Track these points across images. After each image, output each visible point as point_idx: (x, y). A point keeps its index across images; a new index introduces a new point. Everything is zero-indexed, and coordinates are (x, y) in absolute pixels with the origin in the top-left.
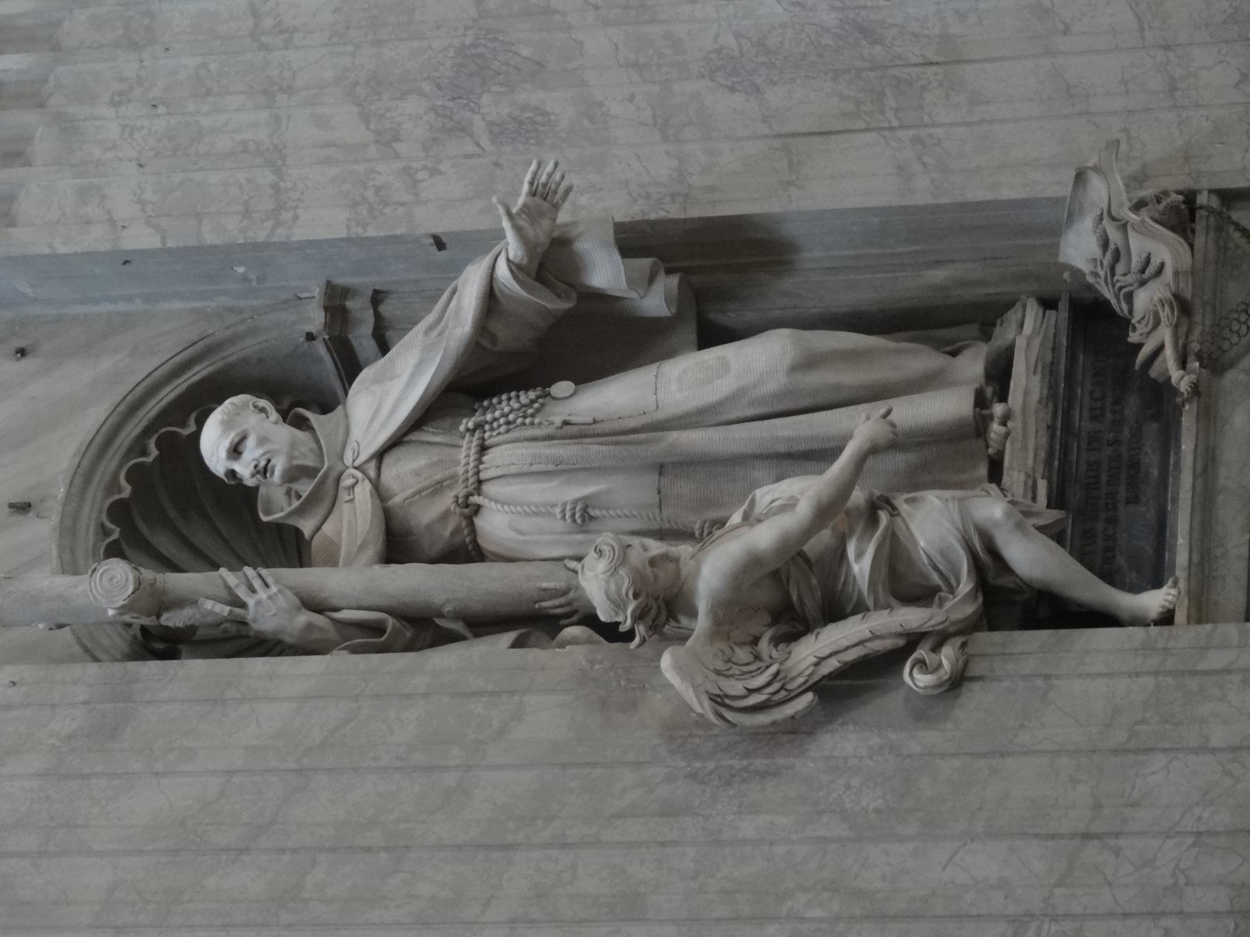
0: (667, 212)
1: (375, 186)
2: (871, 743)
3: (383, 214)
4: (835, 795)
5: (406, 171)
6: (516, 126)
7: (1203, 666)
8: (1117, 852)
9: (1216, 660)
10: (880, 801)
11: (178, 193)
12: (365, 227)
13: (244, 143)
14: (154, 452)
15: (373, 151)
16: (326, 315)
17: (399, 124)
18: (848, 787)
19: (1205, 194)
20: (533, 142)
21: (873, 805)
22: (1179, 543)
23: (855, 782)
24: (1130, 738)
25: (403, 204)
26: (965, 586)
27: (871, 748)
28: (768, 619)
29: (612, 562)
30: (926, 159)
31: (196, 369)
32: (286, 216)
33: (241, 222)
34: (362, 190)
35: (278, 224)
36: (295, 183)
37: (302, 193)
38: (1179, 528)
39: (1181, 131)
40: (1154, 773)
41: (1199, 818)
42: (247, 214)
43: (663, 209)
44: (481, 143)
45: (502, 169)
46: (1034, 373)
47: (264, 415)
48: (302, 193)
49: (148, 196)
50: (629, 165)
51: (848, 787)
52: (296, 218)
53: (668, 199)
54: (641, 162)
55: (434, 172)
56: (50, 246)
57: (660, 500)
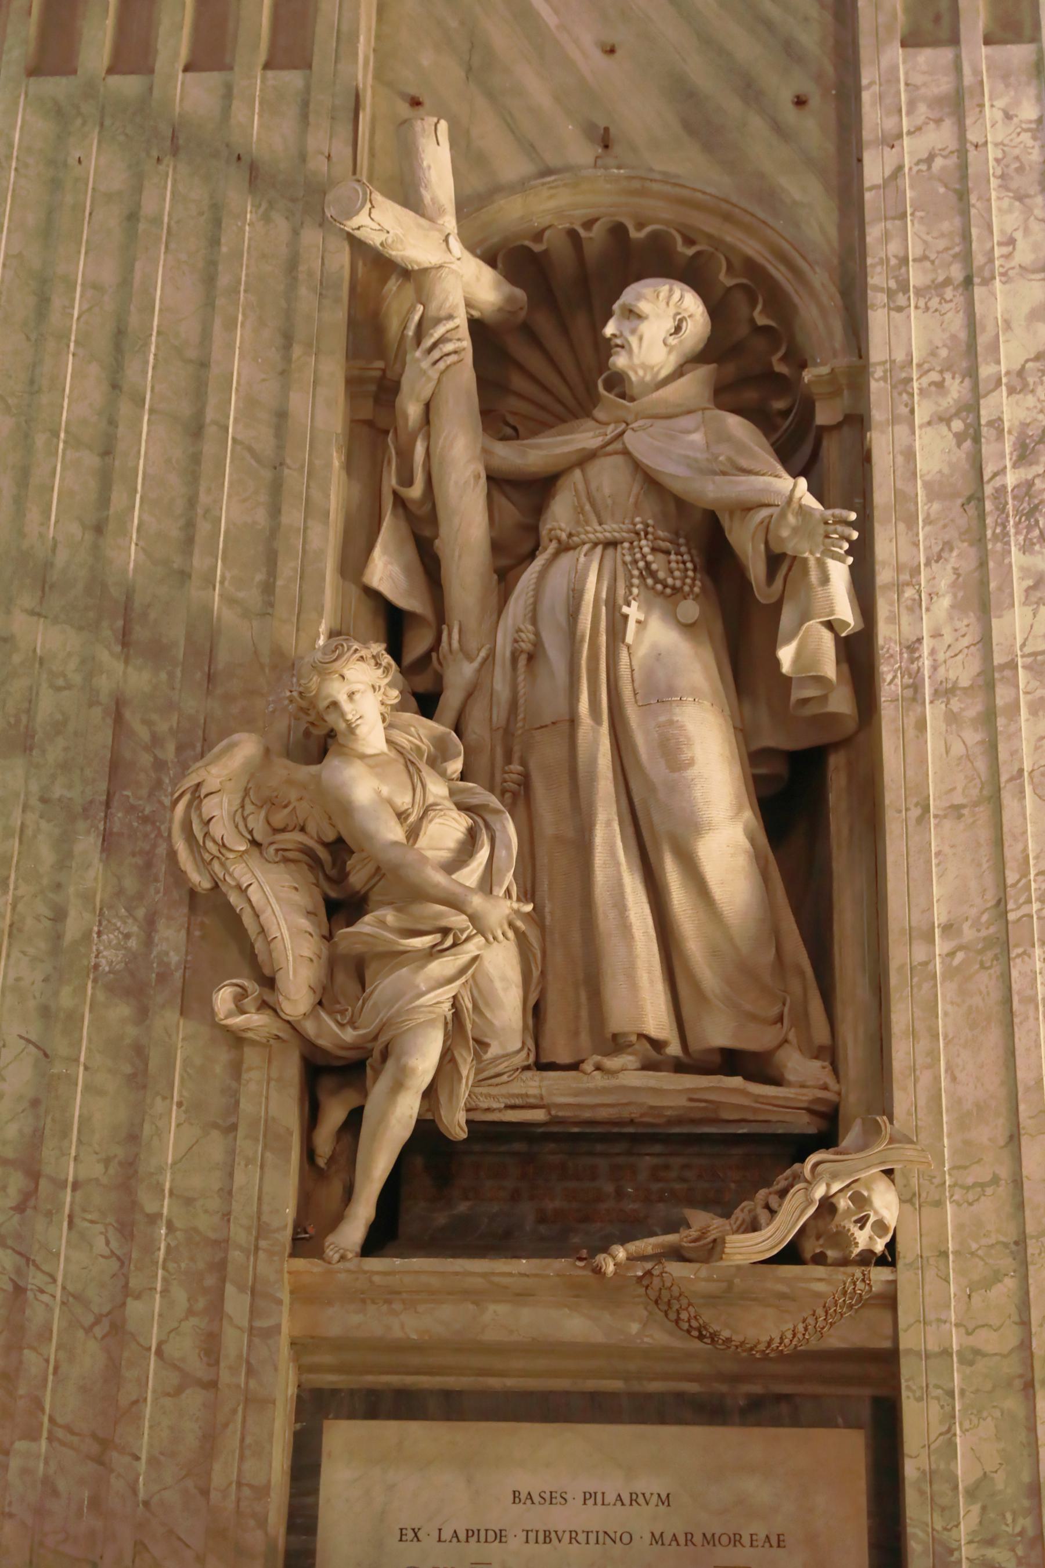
0: (890, 683)
1: (944, 380)
2: (172, 953)
3: (900, 394)
4: (119, 924)
6: (1025, 512)
7: (230, 1289)
10: (107, 969)
14: (690, 252)
16: (828, 374)
17: (1033, 391)
18: (127, 936)
19: (891, 1277)
20: (998, 530)
21: (103, 962)
22: (395, 1259)
23: (133, 943)
24: (148, 1215)
26: (349, 1035)
27: (167, 954)
28: (330, 836)
29: (321, 662)
30: (960, 956)
31: (782, 268)
33: (895, 257)
34: (938, 368)
36: (951, 301)
37: (936, 310)
38: (415, 1260)
39: (992, 1246)
40: (108, 1243)
41: (42, 1291)
43: (895, 677)
44: (998, 478)
46: (691, 1100)
48: (936, 310)
50: (964, 636)
51: (127, 936)
53: (907, 680)
54: (968, 647)
56: (871, 84)
57: (546, 726)
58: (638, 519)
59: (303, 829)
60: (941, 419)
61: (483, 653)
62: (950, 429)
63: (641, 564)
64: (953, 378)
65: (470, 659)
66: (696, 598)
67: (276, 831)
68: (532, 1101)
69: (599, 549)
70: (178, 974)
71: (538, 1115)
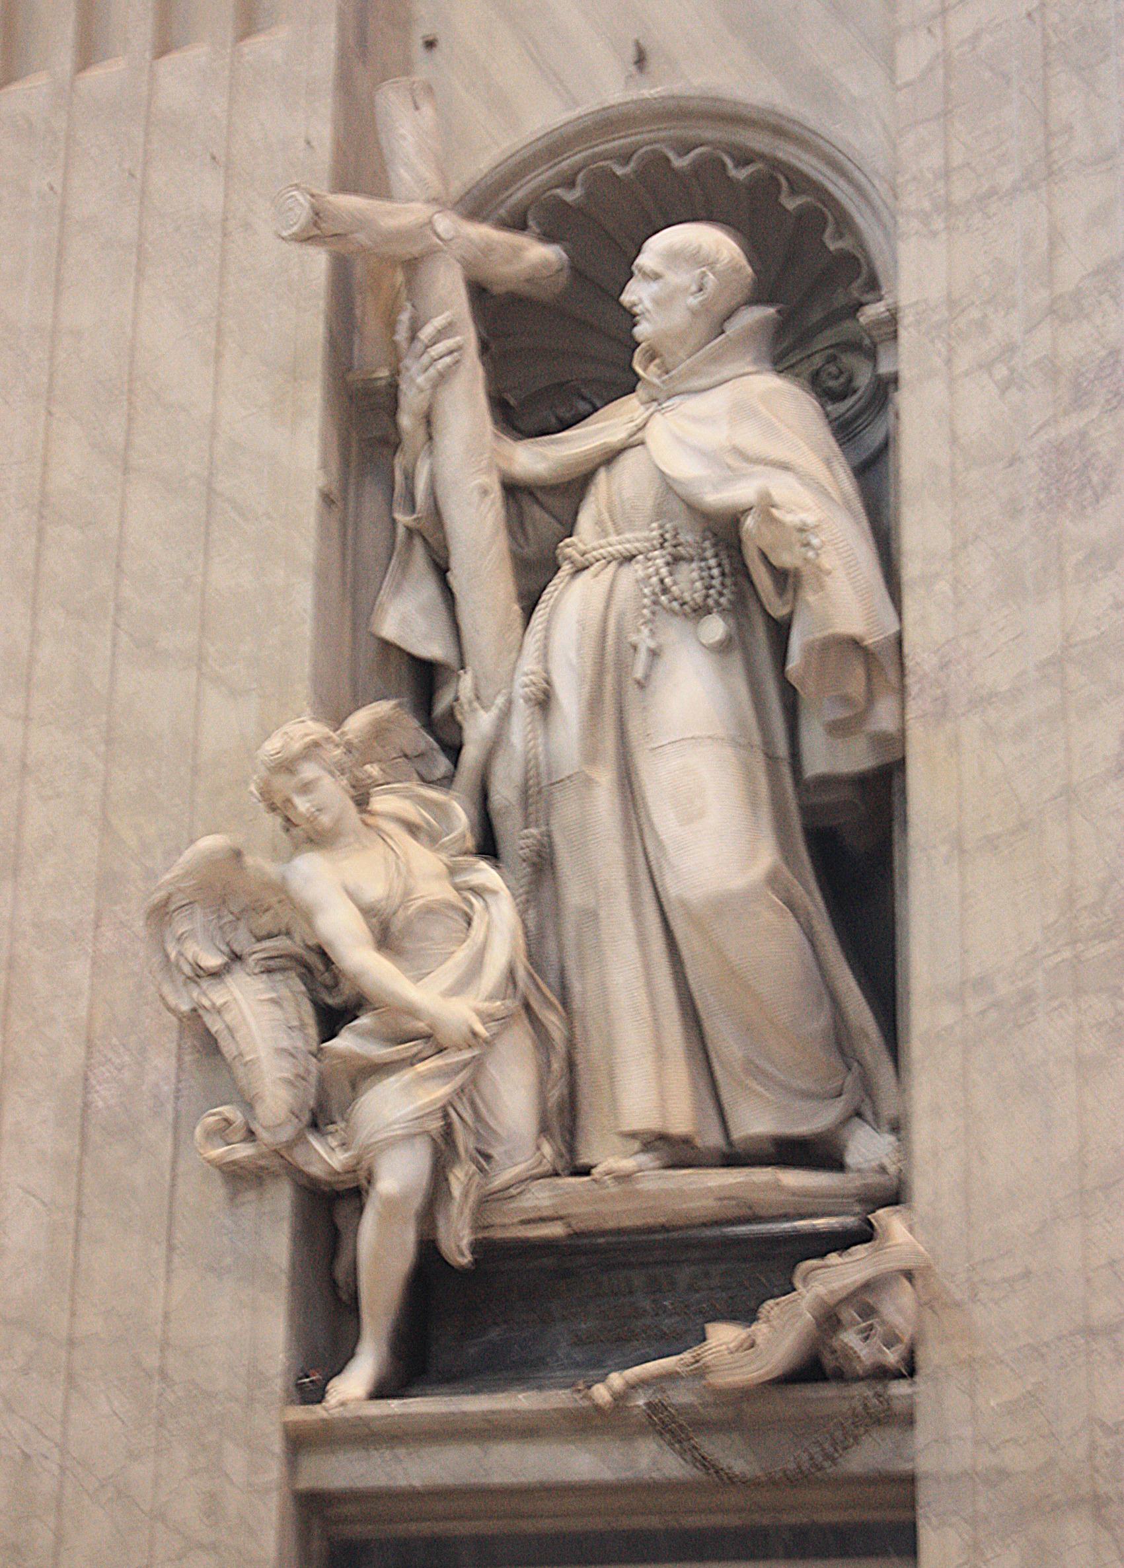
1: (985, 316)
5: (1010, 349)
7: (228, 1445)
8: (25, 1371)
9: (235, 1460)
11: (987, 75)
12: (918, 323)
13: (1069, 128)
15: (1042, 296)
25: (949, 362)
27: (157, 1085)
30: (993, 1015)
32: (938, 224)
35: (925, 217)
42: (946, 174)
45: (1005, 468)
47: (694, 288)
49: (987, 40)
52: (934, 234)
55: (1005, 387)
58: (654, 525)
59: (288, 933)
60: (981, 367)
61: (500, 701)
62: (991, 375)
63: (655, 580)
64: (996, 311)
65: (486, 708)
66: (723, 612)
67: (259, 939)
68: (545, 1214)
69: (614, 564)
70: (169, 1107)
71: (556, 1230)
